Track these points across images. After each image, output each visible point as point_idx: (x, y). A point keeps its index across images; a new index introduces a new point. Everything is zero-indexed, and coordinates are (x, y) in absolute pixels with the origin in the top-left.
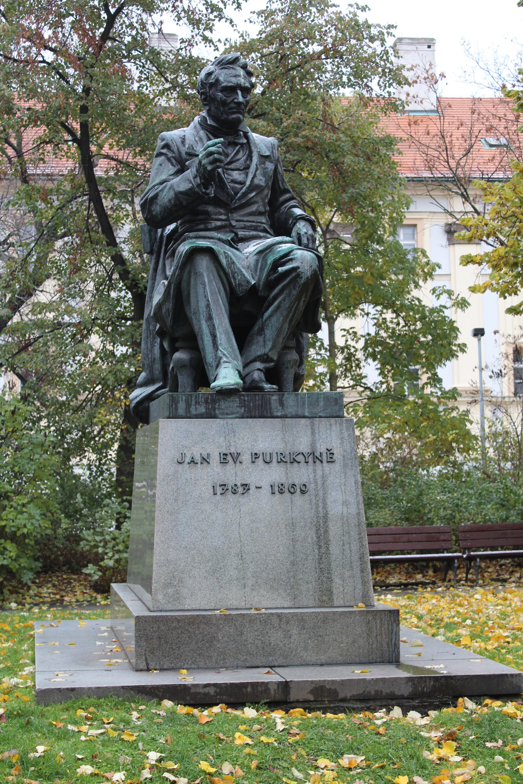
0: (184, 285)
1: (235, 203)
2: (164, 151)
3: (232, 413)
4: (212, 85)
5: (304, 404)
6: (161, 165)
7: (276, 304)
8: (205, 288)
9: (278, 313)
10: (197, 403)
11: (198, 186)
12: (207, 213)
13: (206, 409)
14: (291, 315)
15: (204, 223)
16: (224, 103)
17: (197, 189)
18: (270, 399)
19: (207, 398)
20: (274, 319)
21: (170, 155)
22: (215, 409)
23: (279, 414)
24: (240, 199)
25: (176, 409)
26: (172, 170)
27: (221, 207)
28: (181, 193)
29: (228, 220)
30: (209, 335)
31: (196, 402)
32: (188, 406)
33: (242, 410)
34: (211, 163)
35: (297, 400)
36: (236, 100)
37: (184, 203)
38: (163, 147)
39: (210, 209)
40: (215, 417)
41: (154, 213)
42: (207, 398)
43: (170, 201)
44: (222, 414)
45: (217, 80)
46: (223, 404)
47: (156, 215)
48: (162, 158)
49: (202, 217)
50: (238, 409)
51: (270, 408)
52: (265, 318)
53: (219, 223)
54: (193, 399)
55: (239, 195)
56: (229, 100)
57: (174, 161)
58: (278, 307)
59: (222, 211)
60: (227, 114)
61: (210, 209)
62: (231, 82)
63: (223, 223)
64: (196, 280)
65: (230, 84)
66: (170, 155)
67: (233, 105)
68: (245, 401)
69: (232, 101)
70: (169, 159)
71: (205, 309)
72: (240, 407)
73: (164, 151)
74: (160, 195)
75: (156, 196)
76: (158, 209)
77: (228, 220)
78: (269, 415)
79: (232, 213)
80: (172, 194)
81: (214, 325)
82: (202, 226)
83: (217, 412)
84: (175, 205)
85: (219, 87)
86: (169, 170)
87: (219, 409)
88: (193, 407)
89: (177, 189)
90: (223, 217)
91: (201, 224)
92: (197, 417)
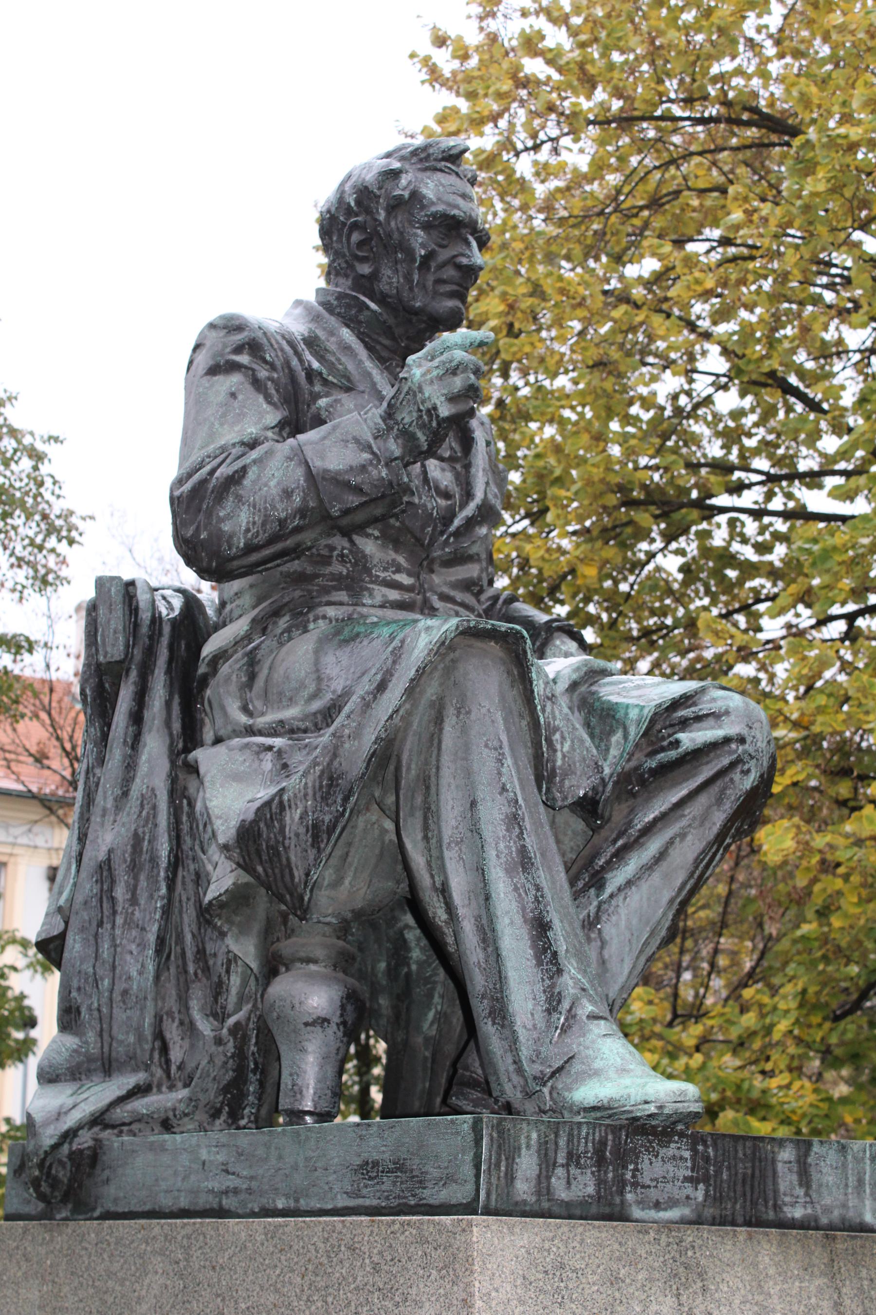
2: (244, 359)
3: (673, 1203)
4: (396, 205)
5: (860, 1182)
6: (233, 395)
7: (653, 846)
9: (656, 877)
10: (573, 1158)
13: (600, 1183)
14: (692, 881)
18: (774, 1161)
19: (603, 1143)
20: (636, 897)
22: (622, 1184)
23: (798, 1213)
24: (457, 534)
25: (510, 1178)
29: (419, 588)
31: (570, 1155)
32: (547, 1165)
33: (700, 1195)
35: (844, 1166)
36: (464, 261)
38: (238, 350)
40: (620, 1215)
42: (603, 1143)
43: (287, 494)
44: (642, 1203)
45: (416, 195)
46: (651, 1168)
48: (236, 379)
50: (689, 1189)
51: (776, 1191)
52: (609, 889)
53: (394, 595)
54: (562, 1142)
55: (457, 522)
58: (661, 857)
62: (457, 207)
63: (407, 596)
65: (455, 212)
68: (707, 1159)
69: (452, 262)
70: (257, 384)
71: (502, 831)
72: (693, 1181)
73: (244, 359)
74: (251, 474)
75: (236, 479)
76: (244, 517)
77: (419, 588)
78: (771, 1215)
83: (629, 1197)
86: (261, 415)
87: (635, 1185)
88: (560, 1171)
90: (404, 579)
92: (570, 1212)
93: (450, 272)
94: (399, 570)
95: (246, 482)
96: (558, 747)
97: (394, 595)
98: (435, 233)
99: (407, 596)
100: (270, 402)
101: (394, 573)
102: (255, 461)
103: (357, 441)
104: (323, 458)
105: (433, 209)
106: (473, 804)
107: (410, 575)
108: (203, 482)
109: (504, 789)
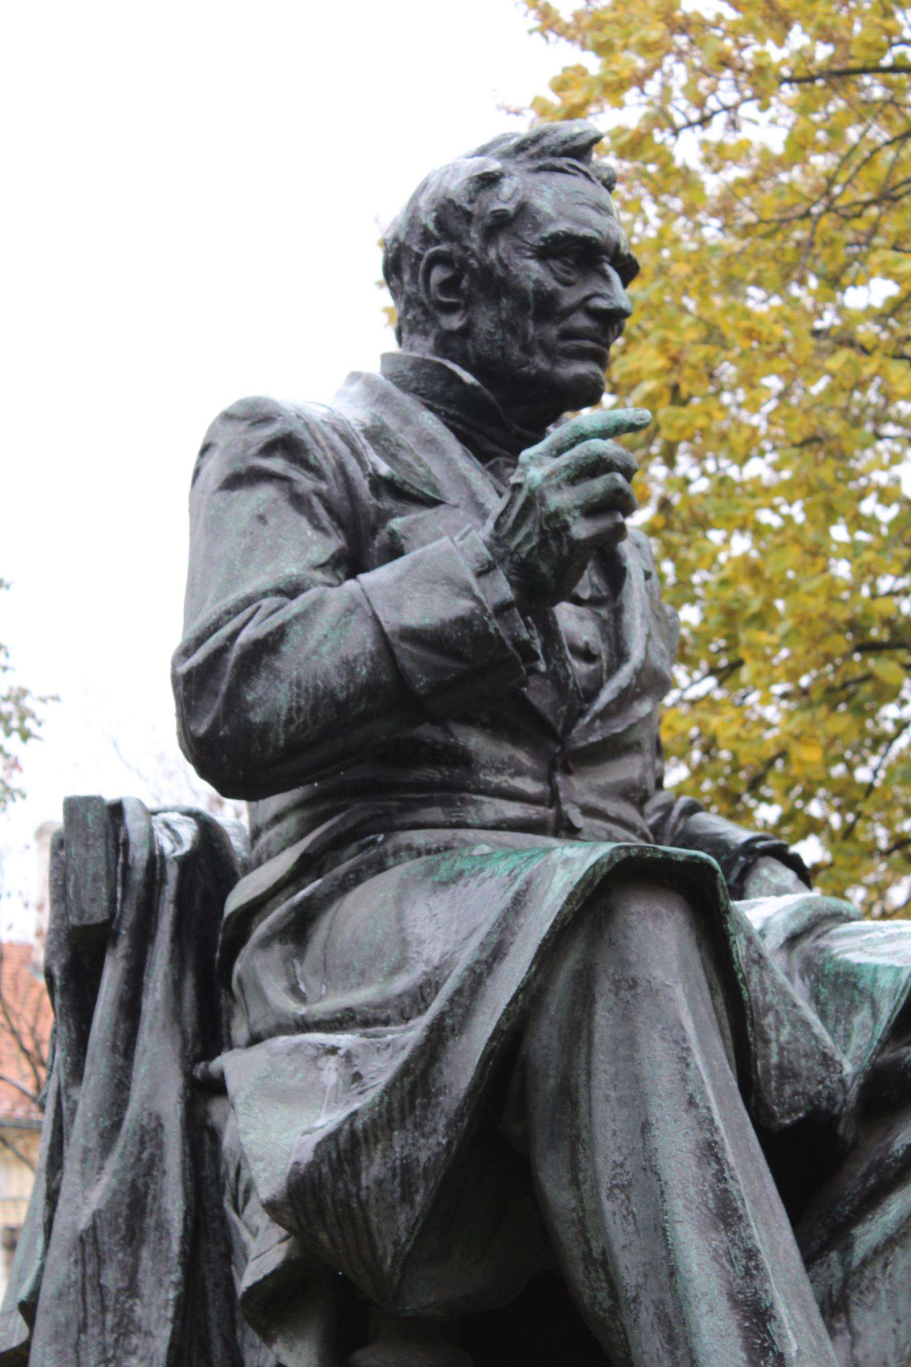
0: (546, 1037)
1: (589, 727)
2: (276, 464)
4: (501, 224)
6: (262, 519)
8: (684, 1061)
11: (502, 609)
12: (463, 760)
15: (445, 803)
16: (545, 306)
17: (494, 625)
21: (305, 482)
24: (606, 714)
26: (326, 546)
27: (516, 739)
28: (411, 635)
30: (723, 1305)
34: (591, 510)
37: (421, 682)
38: (269, 449)
39: (475, 741)
41: (257, 717)
43: (348, 666)
47: (266, 727)
48: (265, 493)
49: (434, 774)
52: (860, 1250)
53: (514, 810)
55: (606, 696)
56: (570, 297)
57: (320, 510)
59: (523, 757)
60: (550, 353)
61: (475, 741)
62: (586, 223)
63: (532, 812)
64: (626, 1017)
66: (305, 482)
67: (581, 321)
69: (583, 306)
70: (298, 501)
73: (276, 464)
75: (268, 646)
77: (553, 799)
79: (568, 772)
80: (360, 640)
81: (751, 1254)
82: (436, 814)
84: (370, 690)
85: (534, 239)
86: (305, 546)
89: (391, 620)
91: (428, 803)
93: (581, 321)
94: (519, 772)
95: (285, 649)
96: (772, 1035)
97: (514, 810)
98: (556, 264)
99: (532, 812)
100: (318, 527)
101: (512, 776)
102: (297, 617)
103: (449, 581)
104: (398, 608)
105: (552, 229)
106: (646, 1127)
107: (536, 778)
108: (220, 653)
109: (691, 1103)
